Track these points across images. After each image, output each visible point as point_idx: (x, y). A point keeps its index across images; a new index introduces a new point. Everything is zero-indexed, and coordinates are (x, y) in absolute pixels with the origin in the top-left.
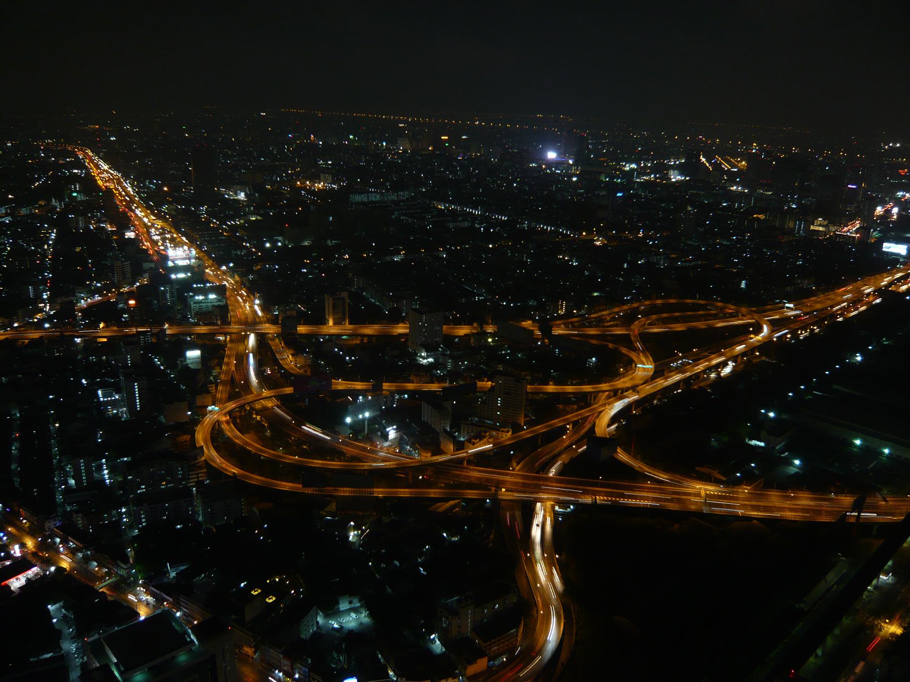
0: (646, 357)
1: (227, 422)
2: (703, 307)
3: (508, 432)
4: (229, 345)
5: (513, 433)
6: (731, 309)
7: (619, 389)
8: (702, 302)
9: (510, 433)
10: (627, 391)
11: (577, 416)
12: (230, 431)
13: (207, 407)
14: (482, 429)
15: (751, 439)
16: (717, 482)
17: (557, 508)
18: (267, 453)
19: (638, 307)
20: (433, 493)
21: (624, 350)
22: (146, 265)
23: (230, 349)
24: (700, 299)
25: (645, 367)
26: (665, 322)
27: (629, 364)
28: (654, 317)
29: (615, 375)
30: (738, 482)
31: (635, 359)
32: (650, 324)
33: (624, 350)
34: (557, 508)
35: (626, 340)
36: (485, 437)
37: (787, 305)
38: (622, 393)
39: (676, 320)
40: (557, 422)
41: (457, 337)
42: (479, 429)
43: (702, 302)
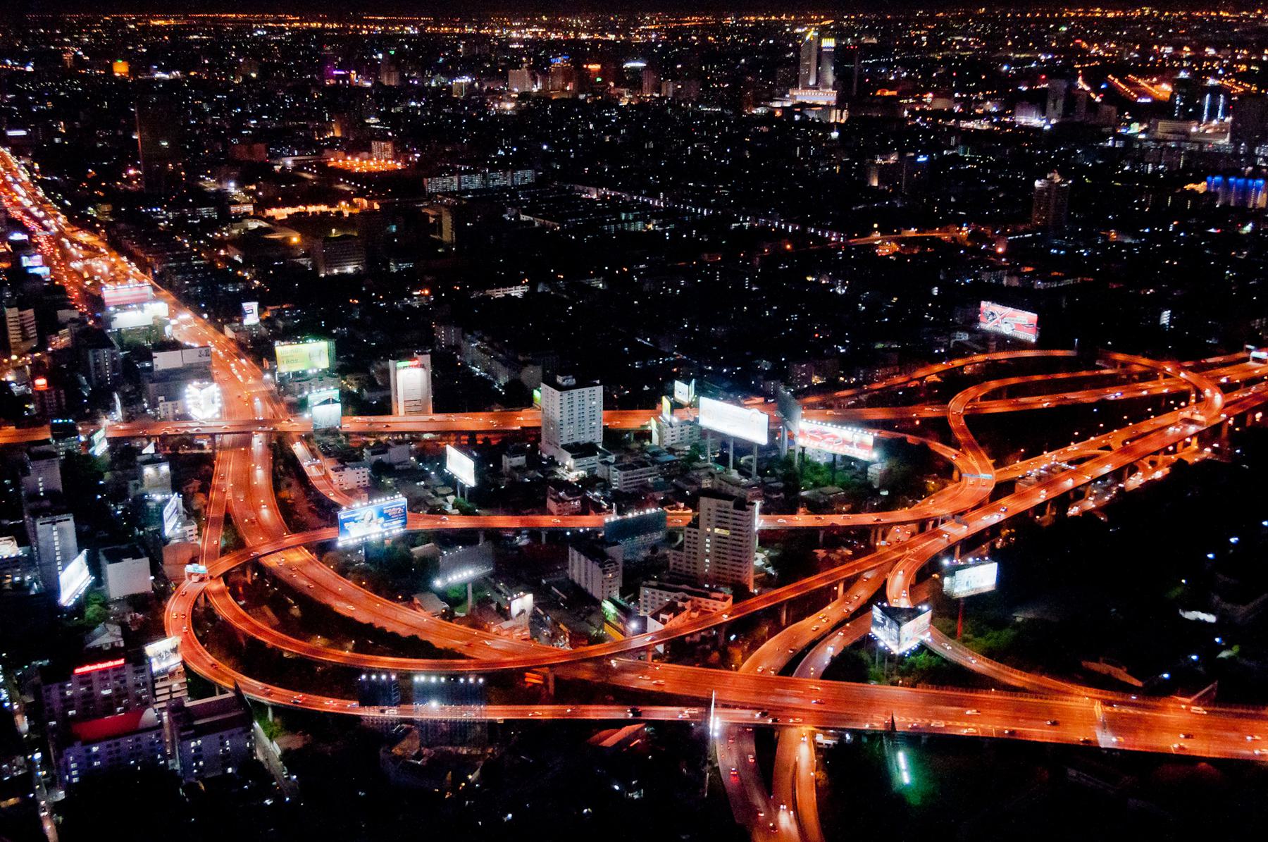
0: (980, 459)
1: (221, 593)
3: (725, 599)
5: (735, 602)
6: (1142, 363)
7: (929, 519)
9: (730, 601)
10: (943, 522)
11: (853, 568)
12: (227, 608)
14: (680, 595)
17: (820, 738)
18: (291, 648)
19: (961, 368)
21: (937, 446)
22: (64, 314)
26: (1013, 392)
28: (994, 384)
29: (920, 492)
30: (1166, 691)
31: (958, 463)
32: (984, 398)
33: (937, 446)
36: (683, 609)
37: (1255, 354)
38: (935, 525)
39: (1037, 390)
40: (815, 582)
42: (673, 595)
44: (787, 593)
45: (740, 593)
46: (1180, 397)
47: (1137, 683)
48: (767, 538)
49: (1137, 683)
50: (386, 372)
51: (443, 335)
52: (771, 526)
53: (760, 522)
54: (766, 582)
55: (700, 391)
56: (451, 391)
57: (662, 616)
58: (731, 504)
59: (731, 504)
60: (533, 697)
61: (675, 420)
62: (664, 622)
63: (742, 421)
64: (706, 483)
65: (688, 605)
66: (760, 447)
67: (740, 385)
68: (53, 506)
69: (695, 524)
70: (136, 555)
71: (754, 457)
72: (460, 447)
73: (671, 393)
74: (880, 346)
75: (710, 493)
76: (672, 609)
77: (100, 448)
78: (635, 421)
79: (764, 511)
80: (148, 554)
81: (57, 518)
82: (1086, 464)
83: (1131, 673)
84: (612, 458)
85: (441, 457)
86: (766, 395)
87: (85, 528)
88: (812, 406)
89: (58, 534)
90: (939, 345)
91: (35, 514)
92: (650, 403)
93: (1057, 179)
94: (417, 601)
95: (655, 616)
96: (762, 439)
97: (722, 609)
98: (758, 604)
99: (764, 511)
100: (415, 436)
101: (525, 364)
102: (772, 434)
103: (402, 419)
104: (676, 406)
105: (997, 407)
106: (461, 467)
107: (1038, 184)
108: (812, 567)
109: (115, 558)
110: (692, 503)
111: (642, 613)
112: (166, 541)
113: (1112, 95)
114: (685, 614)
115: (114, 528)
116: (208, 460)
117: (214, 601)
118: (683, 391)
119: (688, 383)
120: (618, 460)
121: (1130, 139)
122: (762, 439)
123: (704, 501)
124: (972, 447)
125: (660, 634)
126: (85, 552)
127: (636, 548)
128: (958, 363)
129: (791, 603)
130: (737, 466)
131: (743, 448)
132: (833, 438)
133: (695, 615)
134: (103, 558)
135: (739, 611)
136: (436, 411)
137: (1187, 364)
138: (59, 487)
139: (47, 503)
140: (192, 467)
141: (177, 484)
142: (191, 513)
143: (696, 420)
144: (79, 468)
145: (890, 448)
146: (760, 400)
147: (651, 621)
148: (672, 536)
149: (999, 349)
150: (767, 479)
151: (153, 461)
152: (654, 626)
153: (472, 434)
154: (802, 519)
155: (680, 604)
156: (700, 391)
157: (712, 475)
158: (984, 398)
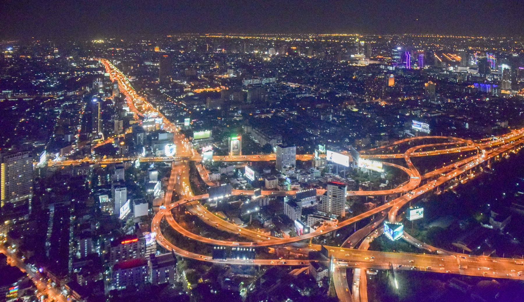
2: (446, 141)
4: (173, 168)
6: (461, 141)
8: (445, 137)
9: (337, 222)
10: (405, 193)
13: (159, 206)
14: (321, 219)
15: (484, 224)
16: (467, 252)
17: (368, 272)
20: (293, 262)
21: (402, 168)
23: (174, 170)
24: (443, 135)
25: (415, 177)
26: (424, 150)
27: (406, 177)
34: (368, 272)
35: (402, 162)
37: (494, 138)
38: (403, 195)
39: (431, 149)
41: (303, 162)
42: (318, 219)
43: (445, 137)
44: (356, 219)
45: (341, 219)
46: (474, 153)
47: (469, 250)
48: (350, 199)
49: (469, 250)
50: (227, 141)
51: (246, 129)
52: (351, 195)
53: (347, 194)
54: (348, 215)
55: (327, 148)
56: (248, 147)
57: (315, 227)
58: (337, 187)
59: (337, 187)
60: (275, 256)
61: (319, 158)
62: (315, 229)
63: (340, 159)
64: (329, 180)
65: (323, 223)
66: (346, 167)
67: (340, 147)
68: (121, 184)
69: (325, 194)
70: (144, 202)
71: (344, 171)
72: (249, 166)
73: (318, 149)
74: (382, 134)
75: (331, 183)
76: (318, 224)
77: (138, 165)
78: (306, 157)
79: (348, 190)
80: (148, 201)
81: (121, 189)
82: (448, 174)
83: (468, 247)
84: (299, 171)
85: (243, 171)
86: (348, 150)
87: (130, 192)
88: (363, 154)
89: (120, 194)
90: (401, 134)
91: (115, 187)
92: (311, 152)
93: (432, 83)
94: (233, 221)
95: (313, 227)
96: (347, 165)
97: (334, 224)
98: (347, 223)
99: (348, 190)
100: (235, 163)
101: (271, 139)
102: (351, 163)
103: (231, 157)
104: (320, 153)
105: (418, 154)
106: (250, 173)
107: (426, 84)
108: (364, 209)
109: (138, 203)
110: (325, 186)
111: (308, 226)
112: (154, 197)
113: (445, 60)
114: (322, 226)
115: (138, 193)
116: (170, 169)
117: (167, 219)
118: (321, 148)
119: (323, 145)
120: (301, 171)
121: (450, 72)
122: (347, 165)
123: (329, 186)
124: (413, 168)
125: (314, 234)
126: (129, 201)
127: (306, 203)
128: (406, 140)
129: (357, 223)
130: (339, 173)
131: (341, 167)
132: (370, 164)
133: (326, 227)
134: (134, 203)
135: (340, 225)
136: (243, 154)
137: (475, 141)
138: (124, 178)
139: (119, 184)
140: (165, 172)
141: (159, 178)
142: (164, 188)
143: (326, 158)
144: (131, 170)
145: (387, 169)
146: (346, 152)
147: (311, 229)
148: (318, 198)
149: (418, 136)
150: (348, 179)
151: (153, 170)
152: (312, 231)
153: (254, 162)
154: (360, 193)
155: (321, 223)
156: (327, 148)
157: (331, 177)
158: (415, 151)
